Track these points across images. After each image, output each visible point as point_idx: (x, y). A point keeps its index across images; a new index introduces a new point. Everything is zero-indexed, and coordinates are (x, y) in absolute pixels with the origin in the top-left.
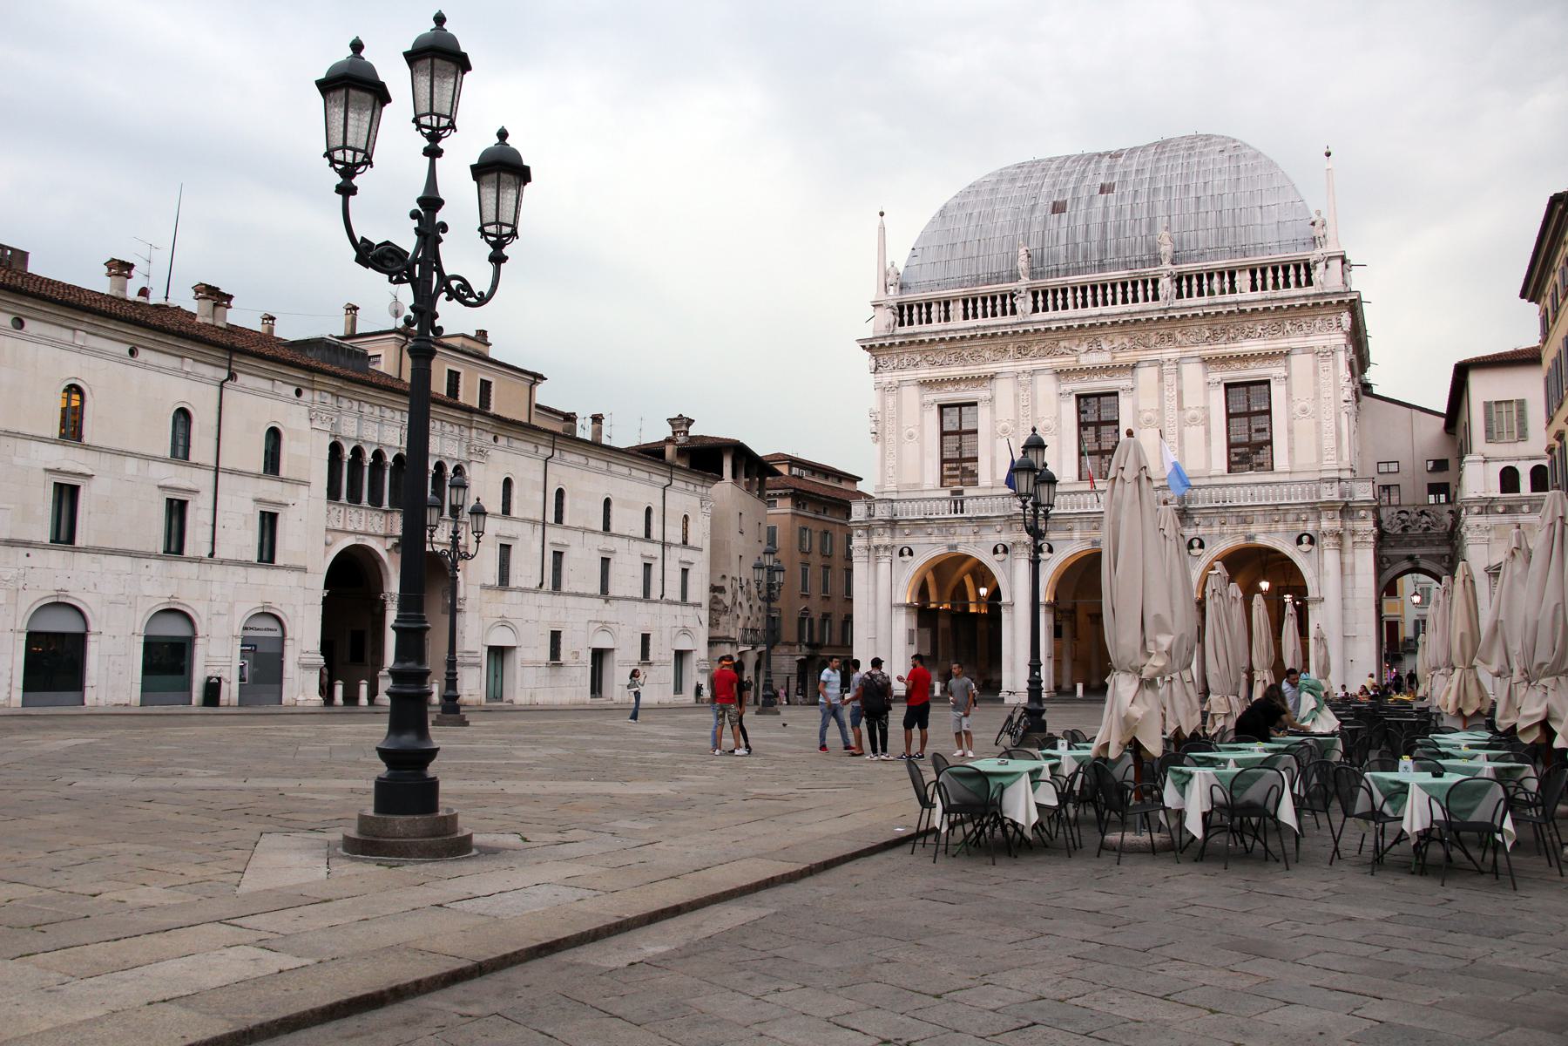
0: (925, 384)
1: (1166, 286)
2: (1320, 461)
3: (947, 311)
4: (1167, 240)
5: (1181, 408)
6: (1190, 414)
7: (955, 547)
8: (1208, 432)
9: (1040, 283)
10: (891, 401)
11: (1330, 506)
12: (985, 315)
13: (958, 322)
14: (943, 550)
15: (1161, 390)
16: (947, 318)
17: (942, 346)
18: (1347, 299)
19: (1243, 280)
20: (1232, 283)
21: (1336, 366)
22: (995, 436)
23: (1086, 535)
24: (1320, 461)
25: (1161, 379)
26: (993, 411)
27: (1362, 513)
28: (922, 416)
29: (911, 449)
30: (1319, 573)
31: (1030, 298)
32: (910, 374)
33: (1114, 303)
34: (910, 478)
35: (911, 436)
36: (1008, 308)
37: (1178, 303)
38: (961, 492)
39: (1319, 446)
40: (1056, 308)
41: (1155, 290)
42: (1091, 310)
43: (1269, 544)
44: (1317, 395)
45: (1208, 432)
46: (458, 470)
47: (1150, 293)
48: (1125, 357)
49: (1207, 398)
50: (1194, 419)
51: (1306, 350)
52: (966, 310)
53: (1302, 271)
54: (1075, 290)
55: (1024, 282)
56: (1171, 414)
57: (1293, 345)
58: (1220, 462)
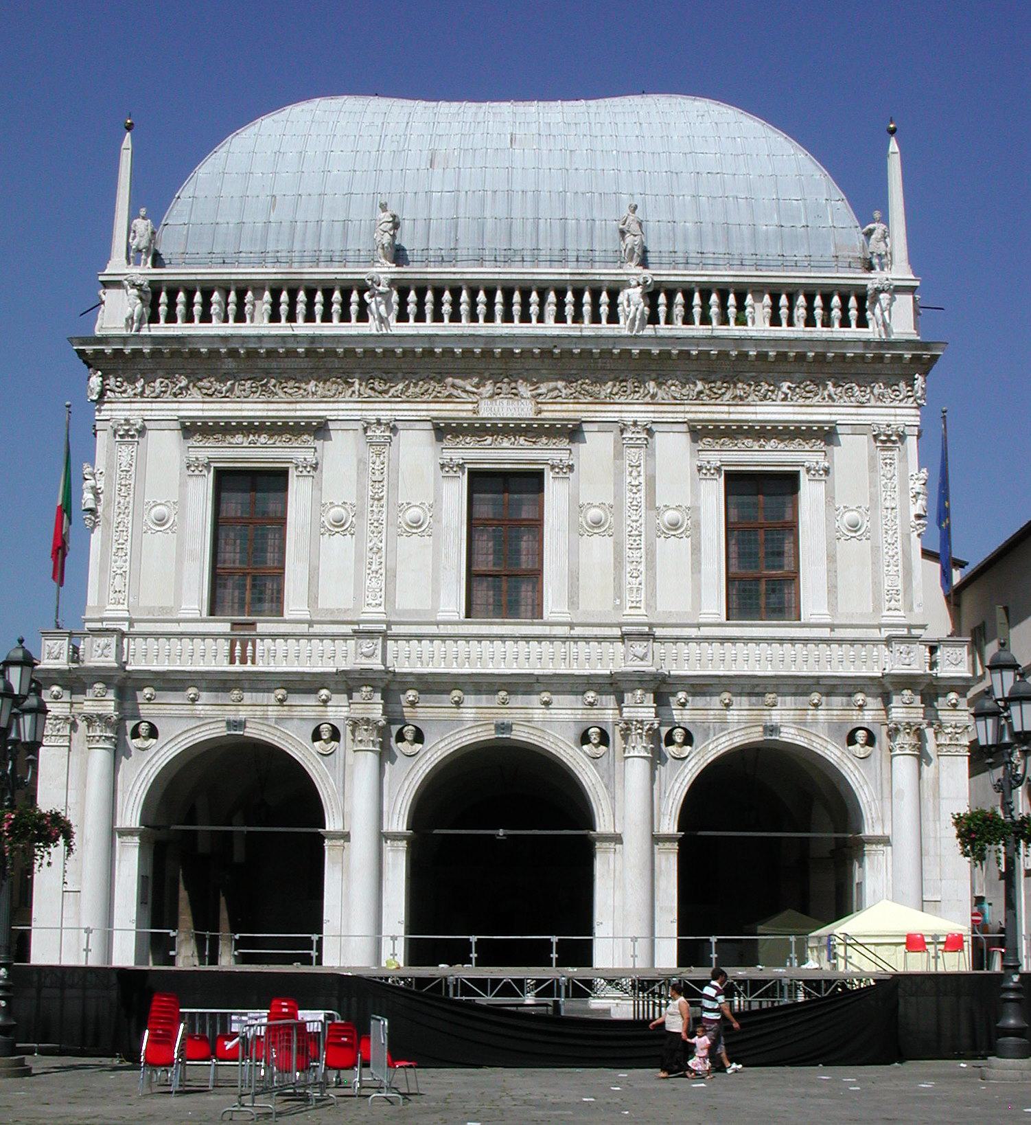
0: (190, 429)
1: (632, 301)
2: (877, 609)
3: (240, 304)
4: (635, 227)
5: (651, 505)
6: (670, 516)
7: (241, 724)
8: (696, 549)
9: (412, 271)
10: (125, 453)
11: (907, 682)
12: (310, 317)
13: (258, 325)
14: (219, 730)
16: (240, 317)
17: (230, 364)
18: (926, 354)
19: (759, 309)
20: (741, 307)
21: (904, 458)
24: (877, 609)
25: (618, 455)
26: (318, 487)
28: (183, 485)
29: (158, 545)
30: (887, 790)
31: (395, 297)
33: (541, 319)
34: (153, 596)
35: (161, 521)
36: (354, 308)
37: (649, 330)
38: (253, 624)
39: (877, 584)
40: (438, 317)
41: (613, 305)
42: (499, 327)
43: (801, 741)
44: (874, 499)
45: (696, 549)
47: (604, 310)
48: (555, 412)
49: (695, 493)
50: (675, 526)
51: (857, 429)
52: (275, 305)
53: (853, 302)
54: (473, 294)
55: (384, 271)
56: (637, 519)
57: (840, 419)
58: (714, 603)
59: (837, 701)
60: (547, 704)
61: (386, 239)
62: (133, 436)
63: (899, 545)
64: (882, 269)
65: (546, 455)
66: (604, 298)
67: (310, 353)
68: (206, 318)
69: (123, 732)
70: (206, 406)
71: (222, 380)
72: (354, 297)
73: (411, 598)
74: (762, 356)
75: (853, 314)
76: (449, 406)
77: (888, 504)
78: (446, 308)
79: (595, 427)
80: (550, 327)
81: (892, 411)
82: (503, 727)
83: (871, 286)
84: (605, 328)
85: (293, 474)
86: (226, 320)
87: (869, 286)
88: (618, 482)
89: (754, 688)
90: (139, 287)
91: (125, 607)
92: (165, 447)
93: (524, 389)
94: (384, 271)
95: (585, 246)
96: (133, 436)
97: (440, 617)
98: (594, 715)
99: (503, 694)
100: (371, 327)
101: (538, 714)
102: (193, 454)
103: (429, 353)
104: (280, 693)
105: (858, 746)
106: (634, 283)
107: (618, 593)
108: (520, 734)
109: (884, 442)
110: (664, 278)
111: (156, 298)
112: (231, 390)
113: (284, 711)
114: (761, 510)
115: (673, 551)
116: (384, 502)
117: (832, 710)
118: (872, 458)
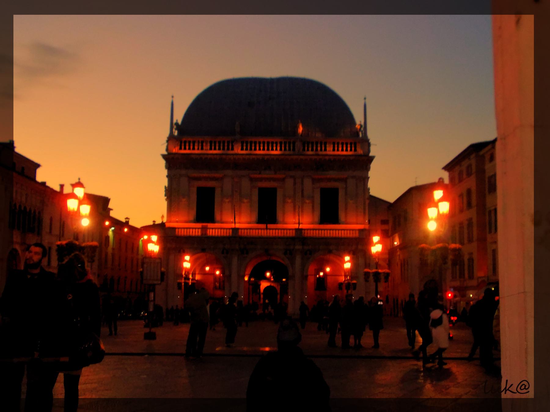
25: (295, 184)
46: (39, 213)
51: (353, 177)
68: (194, 149)
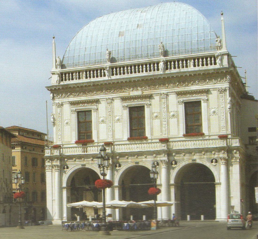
1: (161, 65)
2: (219, 131)
5: (168, 111)
9: (114, 64)
10: (59, 110)
15: (160, 105)
17: (78, 89)
20: (187, 63)
22: (98, 123)
23: (133, 160)
25: (160, 101)
26: (98, 113)
27: (235, 151)
29: (67, 129)
31: (111, 70)
32: (66, 100)
35: (67, 123)
41: (158, 67)
42: (134, 75)
45: (178, 121)
47: (156, 68)
51: (214, 89)
53: (213, 59)
55: (108, 64)
56: (164, 115)
57: (209, 87)
59: (208, 154)
60: (146, 157)
61: (108, 57)
62: (60, 106)
63: (225, 116)
64: (220, 50)
65: (145, 102)
66: (156, 65)
67: (94, 85)
68: (72, 79)
69: (62, 168)
70: (74, 98)
71: (76, 93)
72: (102, 71)
73: (118, 136)
74: (190, 75)
75: (213, 61)
76: (124, 93)
77: (222, 106)
78: (122, 71)
79: (155, 95)
80: (145, 74)
81: (222, 84)
82: (137, 163)
83: (216, 55)
84: (156, 73)
85: (93, 111)
86: (77, 79)
87: (216, 55)
88: (160, 107)
89: (190, 152)
90: (58, 74)
91: (61, 142)
92: (67, 108)
93: (139, 88)
94: (108, 64)
95: (152, 52)
96: (60, 106)
97: (124, 140)
98: (156, 159)
99: (136, 156)
100: (106, 78)
101: (144, 159)
102: (72, 109)
103: (118, 83)
104: (92, 158)
105: (213, 163)
106: (161, 61)
107: (161, 131)
108: (141, 164)
109: (220, 92)
110: (168, 59)
111: (62, 76)
112: (79, 94)
113: (93, 162)
114: (193, 111)
115: (173, 121)
116: (111, 115)
117: (208, 155)
118: (218, 96)
